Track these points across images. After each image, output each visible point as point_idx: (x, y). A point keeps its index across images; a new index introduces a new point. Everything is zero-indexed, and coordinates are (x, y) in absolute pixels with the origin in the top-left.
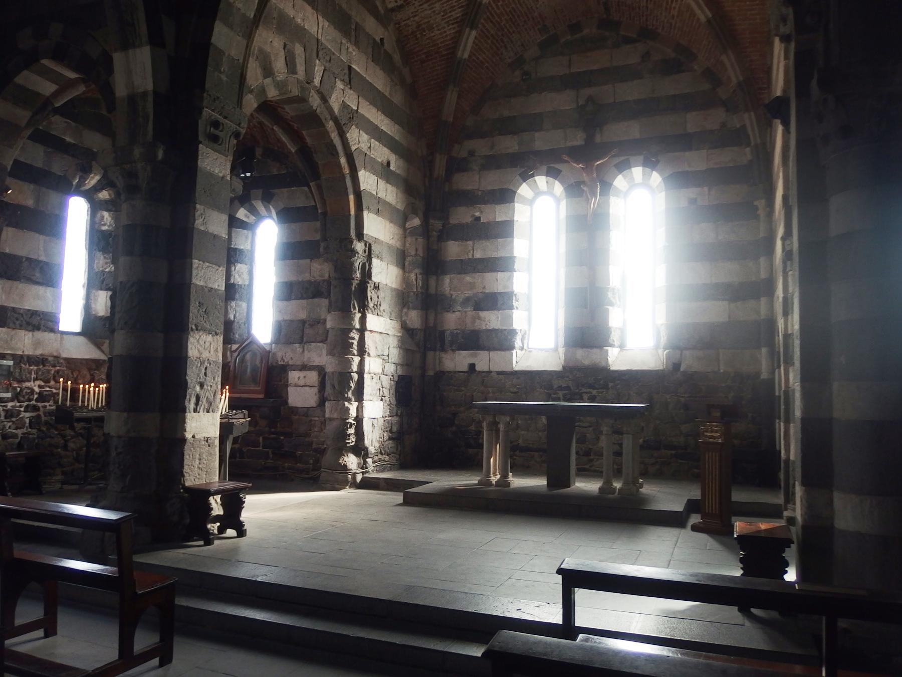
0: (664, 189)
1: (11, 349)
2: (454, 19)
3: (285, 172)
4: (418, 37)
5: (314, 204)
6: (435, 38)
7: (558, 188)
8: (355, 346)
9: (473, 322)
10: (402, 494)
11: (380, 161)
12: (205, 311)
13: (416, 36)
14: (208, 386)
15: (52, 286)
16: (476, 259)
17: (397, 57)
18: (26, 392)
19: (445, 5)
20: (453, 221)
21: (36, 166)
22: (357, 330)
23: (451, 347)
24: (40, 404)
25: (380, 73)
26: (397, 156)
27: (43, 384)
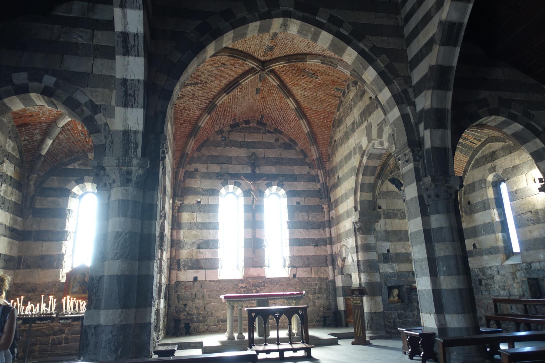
0: (286, 196)
6: (190, 114)
7: (239, 191)
9: (197, 255)
13: (182, 112)
16: (198, 222)
20: (186, 202)
22: (159, 259)
23: (184, 268)
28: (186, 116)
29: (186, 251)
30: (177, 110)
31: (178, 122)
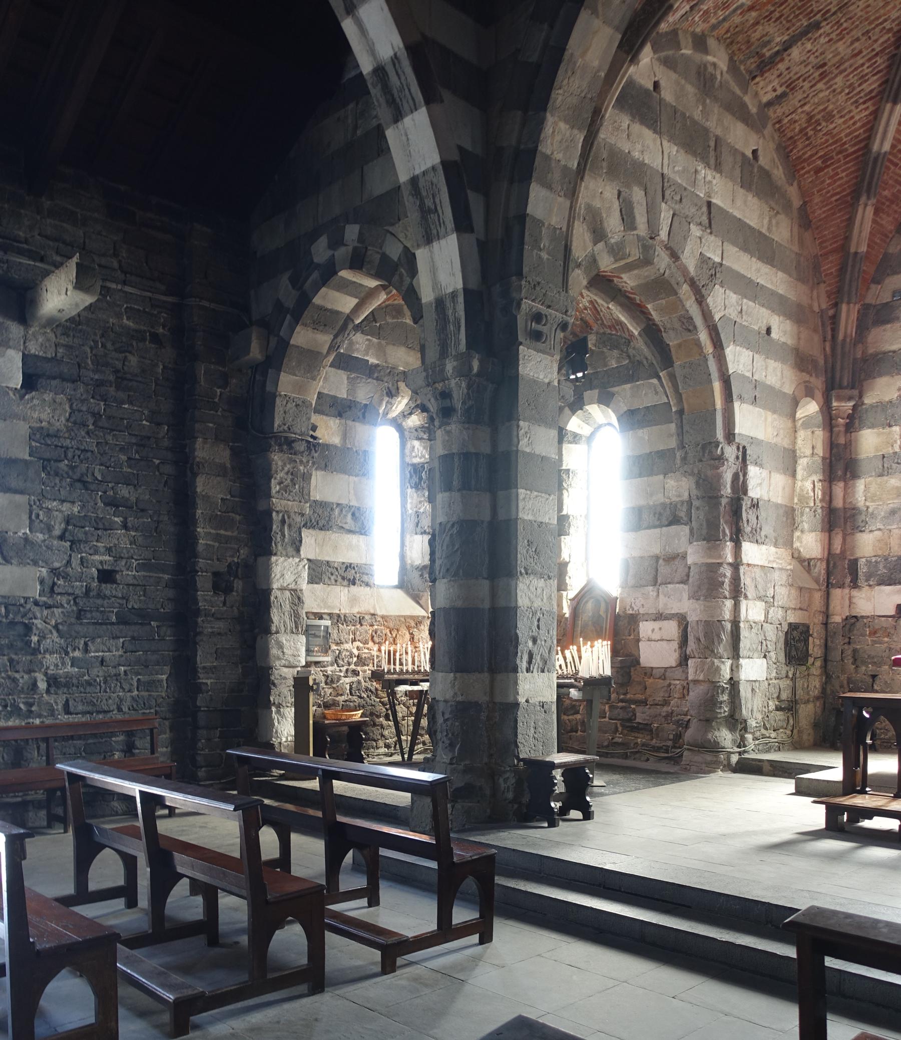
1: (329, 607)
2: (866, 95)
3: (627, 361)
4: (809, 135)
5: (667, 401)
6: (835, 132)
8: (727, 586)
10: (793, 781)
11: (756, 328)
12: (536, 551)
13: (807, 134)
14: (541, 641)
15: (365, 534)
17: (779, 173)
18: (345, 655)
19: (851, 76)
21: (340, 396)
24: (359, 668)
25: (753, 201)
26: (781, 318)
27: (361, 645)
28: (827, 141)
29: (871, 536)
30: (789, 135)
31: (807, 169)
